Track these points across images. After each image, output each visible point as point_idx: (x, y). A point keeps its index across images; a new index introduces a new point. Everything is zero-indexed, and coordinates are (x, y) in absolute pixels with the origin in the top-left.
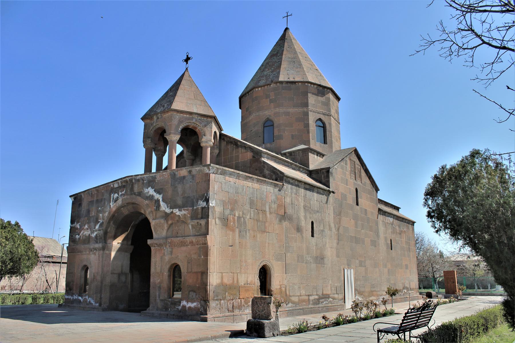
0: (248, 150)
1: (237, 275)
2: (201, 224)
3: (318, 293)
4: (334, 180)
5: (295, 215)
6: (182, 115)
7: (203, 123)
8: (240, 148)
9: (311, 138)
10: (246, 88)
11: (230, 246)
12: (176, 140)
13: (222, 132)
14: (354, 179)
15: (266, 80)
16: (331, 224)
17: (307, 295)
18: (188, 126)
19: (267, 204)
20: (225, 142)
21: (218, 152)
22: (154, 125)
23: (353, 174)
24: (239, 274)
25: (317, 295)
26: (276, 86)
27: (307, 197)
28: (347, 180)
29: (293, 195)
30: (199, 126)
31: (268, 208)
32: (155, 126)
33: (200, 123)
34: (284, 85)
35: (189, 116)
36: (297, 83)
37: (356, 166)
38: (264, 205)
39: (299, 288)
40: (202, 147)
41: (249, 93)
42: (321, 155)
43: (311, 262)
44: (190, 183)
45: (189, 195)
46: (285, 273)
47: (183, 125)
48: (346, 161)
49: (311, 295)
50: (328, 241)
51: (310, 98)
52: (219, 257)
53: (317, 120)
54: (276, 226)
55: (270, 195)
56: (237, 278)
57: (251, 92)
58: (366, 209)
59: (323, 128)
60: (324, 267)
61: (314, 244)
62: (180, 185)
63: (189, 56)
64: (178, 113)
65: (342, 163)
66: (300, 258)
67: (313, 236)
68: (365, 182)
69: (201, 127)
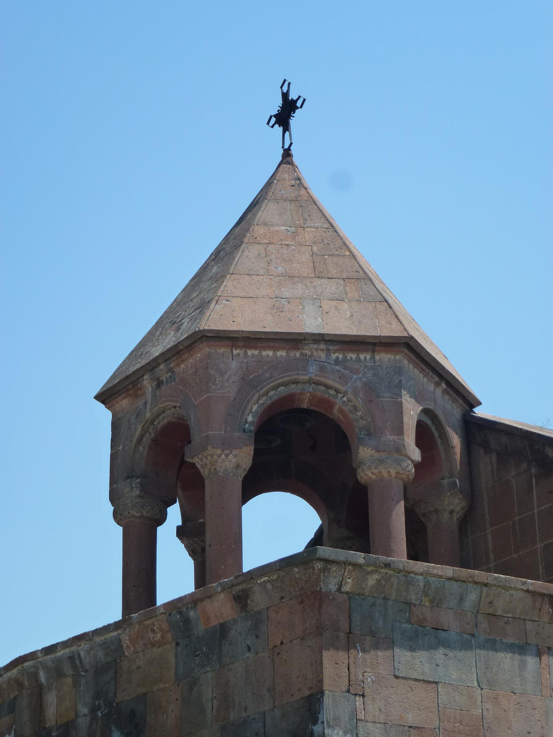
6: (256, 352)
7: (355, 376)
12: (238, 466)
13: (479, 412)
18: (290, 398)
20: (494, 456)
21: (464, 504)
22: (148, 415)
30: (337, 391)
32: (152, 422)
33: (344, 379)
35: (275, 354)
44: (248, 655)
45: (244, 715)
47: (264, 398)
62: (208, 669)
63: (293, 96)
64: (236, 347)
69: (351, 396)
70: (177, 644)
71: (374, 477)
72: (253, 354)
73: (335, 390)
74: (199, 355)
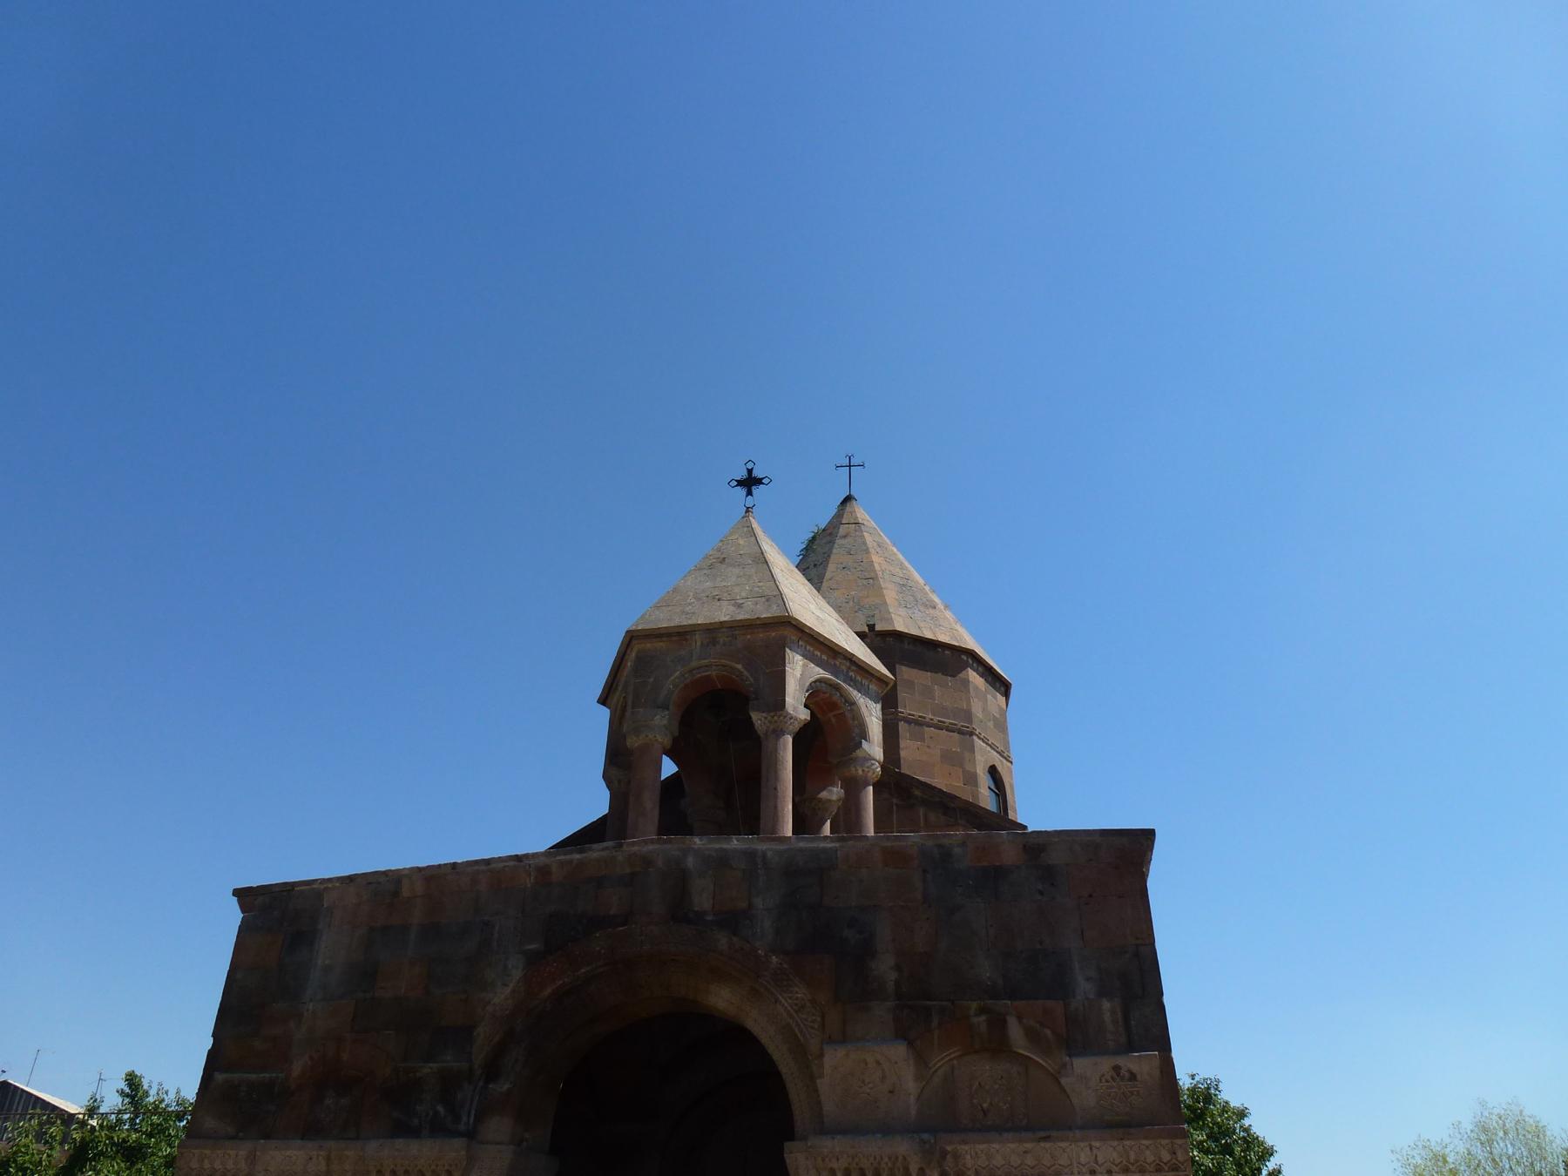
2: (1133, 1077)
6: (812, 649)
8: (921, 811)
22: (694, 664)
26: (882, 645)
70: (925, 871)
72: (809, 651)
74: (773, 634)
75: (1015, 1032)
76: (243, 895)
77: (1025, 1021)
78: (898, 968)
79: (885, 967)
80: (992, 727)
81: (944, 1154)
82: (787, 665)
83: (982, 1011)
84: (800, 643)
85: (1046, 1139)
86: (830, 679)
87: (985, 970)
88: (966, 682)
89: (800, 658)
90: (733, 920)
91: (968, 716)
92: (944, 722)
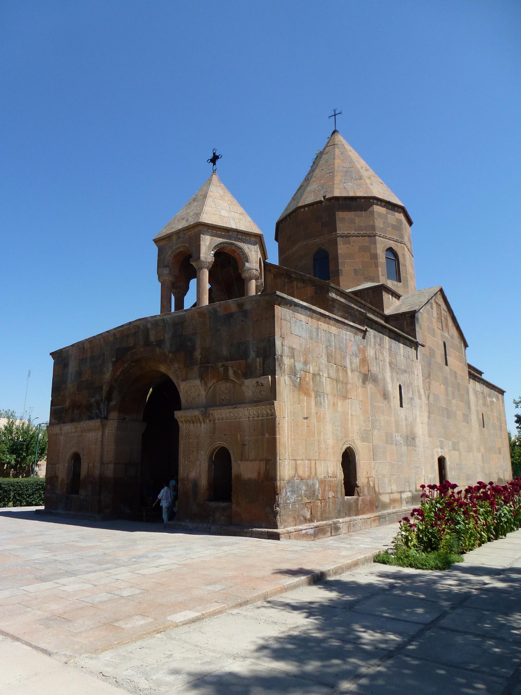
0: (307, 284)
1: (315, 463)
2: (262, 385)
3: (411, 489)
4: (420, 328)
5: (380, 375)
6: (215, 232)
9: (380, 273)
10: (287, 209)
11: (304, 418)
13: (266, 261)
14: (441, 329)
15: (314, 197)
16: (421, 391)
17: (399, 492)
19: (347, 357)
20: (272, 276)
23: (439, 322)
24: (317, 462)
25: (410, 491)
27: (393, 349)
28: (434, 330)
29: (378, 347)
31: (349, 364)
34: (341, 202)
36: (358, 200)
37: (442, 311)
38: (344, 358)
39: (390, 481)
40: (244, 280)
41: (292, 216)
42: (397, 297)
43: (401, 443)
46: (372, 459)
48: (432, 304)
49: (403, 492)
50: (418, 413)
51: (378, 220)
52: (291, 436)
53: (387, 250)
54: (360, 390)
55: (351, 344)
56: (316, 468)
57: (294, 214)
58: (456, 372)
59: (394, 261)
60: (415, 450)
61: (404, 418)
63: (217, 154)
64: (210, 229)
65: (428, 307)
66: (389, 439)
67: (401, 406)
68: (453, 334)
70: (210, 318)
71: (248, 276)
72: (214, 232)
73: (238, 248)
75: (231, 372)
76: (51, 354)
77: (233, 368)
78: (201, 354)
79: (197, 354)
80: (391, 230)
81: (209, 414)
82: (201, 241)
83: (223, 366)
84: (209, 231)
85: (235, 407)
86: (227, 242)
87: (225, 351)
88: (372, 213)
89: (209, 237)
90: (160, 343)
91: (373, 228)
92: (360, 233)
